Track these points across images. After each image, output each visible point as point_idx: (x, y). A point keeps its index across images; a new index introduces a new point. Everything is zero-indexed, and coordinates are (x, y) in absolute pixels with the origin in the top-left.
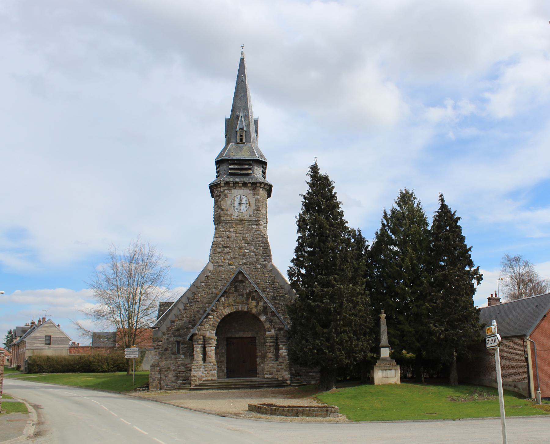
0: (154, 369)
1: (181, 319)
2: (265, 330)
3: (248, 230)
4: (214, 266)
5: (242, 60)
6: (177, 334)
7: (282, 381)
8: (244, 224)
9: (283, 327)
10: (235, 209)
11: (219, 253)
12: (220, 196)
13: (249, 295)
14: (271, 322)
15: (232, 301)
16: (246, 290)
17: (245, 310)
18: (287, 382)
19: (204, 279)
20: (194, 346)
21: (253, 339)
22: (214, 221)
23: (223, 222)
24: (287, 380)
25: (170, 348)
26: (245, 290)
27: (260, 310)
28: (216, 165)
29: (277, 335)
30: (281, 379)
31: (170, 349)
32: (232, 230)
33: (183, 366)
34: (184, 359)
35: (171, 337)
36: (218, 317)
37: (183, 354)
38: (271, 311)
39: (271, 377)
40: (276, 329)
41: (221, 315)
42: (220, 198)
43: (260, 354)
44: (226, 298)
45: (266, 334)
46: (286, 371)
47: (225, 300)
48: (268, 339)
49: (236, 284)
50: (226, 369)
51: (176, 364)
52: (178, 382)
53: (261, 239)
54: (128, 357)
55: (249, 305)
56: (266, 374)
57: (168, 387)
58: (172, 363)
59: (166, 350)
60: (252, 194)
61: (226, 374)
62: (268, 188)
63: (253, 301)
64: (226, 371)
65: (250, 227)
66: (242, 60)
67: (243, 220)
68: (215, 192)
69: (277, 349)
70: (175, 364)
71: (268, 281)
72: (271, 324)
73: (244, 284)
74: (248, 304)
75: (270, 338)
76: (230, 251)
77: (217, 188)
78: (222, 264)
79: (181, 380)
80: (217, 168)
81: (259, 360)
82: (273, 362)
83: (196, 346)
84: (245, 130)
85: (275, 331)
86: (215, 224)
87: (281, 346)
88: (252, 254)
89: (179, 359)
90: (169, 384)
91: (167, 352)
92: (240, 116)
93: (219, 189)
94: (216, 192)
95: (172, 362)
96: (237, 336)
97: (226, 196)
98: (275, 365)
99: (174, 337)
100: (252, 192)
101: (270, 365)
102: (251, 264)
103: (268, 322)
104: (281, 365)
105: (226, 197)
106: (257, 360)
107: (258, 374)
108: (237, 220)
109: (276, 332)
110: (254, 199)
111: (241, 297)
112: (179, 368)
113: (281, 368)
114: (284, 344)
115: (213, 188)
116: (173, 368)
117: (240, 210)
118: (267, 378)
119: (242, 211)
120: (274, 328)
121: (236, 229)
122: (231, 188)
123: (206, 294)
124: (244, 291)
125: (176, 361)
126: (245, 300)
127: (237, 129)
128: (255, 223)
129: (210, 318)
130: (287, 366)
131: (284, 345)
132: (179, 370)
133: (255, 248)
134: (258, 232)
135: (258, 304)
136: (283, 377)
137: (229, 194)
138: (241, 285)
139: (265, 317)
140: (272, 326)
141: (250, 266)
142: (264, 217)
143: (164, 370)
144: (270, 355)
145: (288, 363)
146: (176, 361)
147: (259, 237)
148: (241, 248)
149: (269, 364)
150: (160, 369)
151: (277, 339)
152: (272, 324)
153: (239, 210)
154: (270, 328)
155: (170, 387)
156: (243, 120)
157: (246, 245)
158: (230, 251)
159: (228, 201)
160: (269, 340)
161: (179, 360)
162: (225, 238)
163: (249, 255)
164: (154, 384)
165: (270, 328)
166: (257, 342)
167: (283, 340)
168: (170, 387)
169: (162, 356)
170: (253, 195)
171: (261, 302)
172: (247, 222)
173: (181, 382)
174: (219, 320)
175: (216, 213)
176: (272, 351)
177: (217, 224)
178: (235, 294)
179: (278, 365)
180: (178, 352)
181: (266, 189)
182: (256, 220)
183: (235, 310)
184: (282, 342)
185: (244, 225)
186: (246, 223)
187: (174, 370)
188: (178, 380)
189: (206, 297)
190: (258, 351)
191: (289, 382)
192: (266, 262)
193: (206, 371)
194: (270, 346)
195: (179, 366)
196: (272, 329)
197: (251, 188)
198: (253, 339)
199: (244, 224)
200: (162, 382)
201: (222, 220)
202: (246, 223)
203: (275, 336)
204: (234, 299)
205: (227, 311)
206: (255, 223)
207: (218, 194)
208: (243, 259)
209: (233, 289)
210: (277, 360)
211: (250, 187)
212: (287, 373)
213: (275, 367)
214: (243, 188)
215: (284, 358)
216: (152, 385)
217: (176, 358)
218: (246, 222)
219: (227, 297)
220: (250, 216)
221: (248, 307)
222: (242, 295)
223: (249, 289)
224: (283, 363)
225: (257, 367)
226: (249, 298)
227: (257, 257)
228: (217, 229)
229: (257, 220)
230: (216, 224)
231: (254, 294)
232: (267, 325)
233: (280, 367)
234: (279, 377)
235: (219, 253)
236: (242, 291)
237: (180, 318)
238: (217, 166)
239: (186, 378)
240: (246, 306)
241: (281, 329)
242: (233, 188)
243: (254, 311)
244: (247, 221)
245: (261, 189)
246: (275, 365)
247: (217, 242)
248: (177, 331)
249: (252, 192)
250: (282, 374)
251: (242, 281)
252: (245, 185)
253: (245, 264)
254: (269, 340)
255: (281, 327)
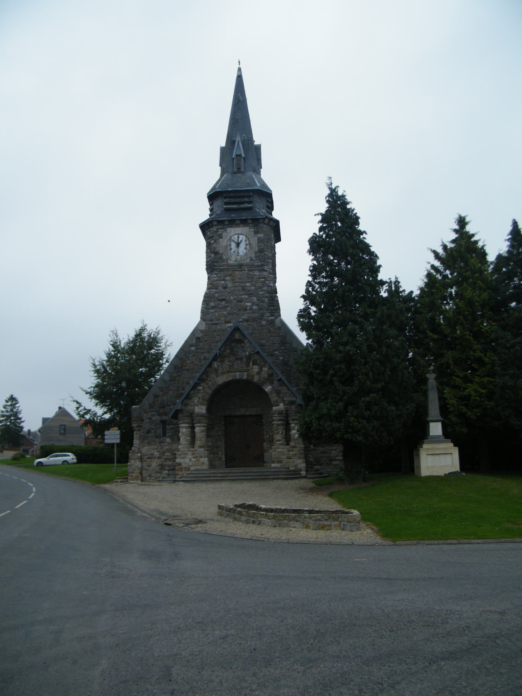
0: (134, 456)
1: (166, 393)
2: (272, 406)
3: (248, 278)
4: (206, 324)
5: (239, 79)
6: (161, 411)
7: (294, 471)
8: (243, 270)
9: (295, 400)
10: (232, 251)
11: (213, 308)
12: (213, 237)
13: (249, 358)
14: (278, 393)
15: (227, 367)
16: (245, 352)
17: (244, 378)
18: (302, 472)
19: (194, 342)
20: (180, 426)
21: (259, 417)
22: (207, 269)
23: (217, 269)
24: (301, 470)
25: (153, 429)
26: (244, 352)
27: (264, 378)
28: (209, 201)
29: (287, 410)
30: (293, 469)
31: (153, 431)
32: (228, 278)
33: (170, 452)
34: (170, 443)
35: (154, 415)
36: (209, 388)
37: (170, 437)
38: (279, 378)
39: (280, 467)
40: (286, 402)
41: (213, 385)
42: (212, 240)
43: (268, 436)
44: (219, 363)
45: (272, 410)
46: (299, 458)
47: (218, 366)
48: (276, 415)
49: (233, 345)
50: (224, 456)
51: (161, 450)
52: (164, 472)
53: (265, 288)
54: (109, 442)
55: (250, 372)
56: (273, 462)
57: (152, 478)
58: (156, 449)
59: (149, 432)
60: (253, 233)
61: (224, 462)
62: (274, 225)
63: (254, 367)
64: (224, 459)
65: (251, 273)
66: (239, 79)
67: (243, 265)
68: (207, 234)
69: (288, 429)
70: (159, 449)
71: (277, 341)
72: (279, 397)
73: (243, 345)
74: (248, 371)
75: (278, 414)
76: (227, 304)
77: (209, 227)
78: (217, 322)
79: (167, 470)
80: (211, 205)
81: (267, 444)
82: (282, 447)
83: (182, 425)
84: (243, 156)
85: (284, 405)
86: (208, 273)
87: (293, 425)
88: (254, 307)
89: (164, 443)
90: (153, 475)
91: (150, 434)
92: (237, 141)
93: (212, 229)
94: (209, 233)
95: (156, 447)
96: (238, 413)
97: (221, 236)
98: (284, 450)
99: (159, 415)
100: (253, 230)
101: (278, 450)
102: (254, 320)
103: (275, 394)
104: (293, 451)
105: (220, 238)
106: (265, 444)
107: (266, 462)
108: (235, 266)
109: (285, 406)
110: (256, 238)
111: (239, 362)
112: (165, 454)
113: (293, 455)
114: (296, 422)
115: (205, 227)
116: (157, 454)
117: (238, 253)
118: (275, 468)
119: (241, 253)
120: (284, 402)
121: (233, 277)
122: (226, 227)
123: (197, 360)
124: (243, 355)
125: (161, 445)
126: (244, 365)
127: (234, 156)
128: (258, 268)
129: (199, 390)
130: (301, 451)
131: (296, 424)
132: (165, 457)
133: (258, 300)
134: (261, 280)
135: (261, 369)
136: (296, 466)
137: (224, 235)
138: (239, 345)
139: (270, 387)
140: (280, 399)
141: (252, 324)
142: (269, 260)
143: (146, 457)
144: (278, 437)
145: (302, 447)
146: (161, 445)
147: (264, 286)
148: (241, 301)
149: (277, 448)
150: (141, 456)
151: (287, 416)
152: (281, 395)
153: (236, 253)
154: (277, 401)
155: (153, 478)
156: (241, 145)
157: (247, 296)
158: (227, 304)
159: (223, 242)
160: (276, 417)
161: (165, 444)
162: (220, 289)
163: (251, 309)
164: (134, 475)
165: (277, 401)
166: (264, 421)
167: (295, 417)
168: (153, 478)
169: (144, 440)
170: (254, 234)
171: (265, 367)
172: (247, 268)
173: (167, 472)
174: (211, 392)
175: (208, 259)
176: (281, 432)
177: (210, 272)
178: (231, 357)
179: (289, 451)
180: (164, 435)
181: (271, 226)
182: (259, 264)
183: (231, 379)
184: (293, 420)
185: (243, 272)
186: (246, 269)
187: (159, 458)
188: (164, 470)
189: (197, 364)
190: (265, 433)
191: (303, 473)
192: (273, 318)
193: (194, 458)
194: (278, 425)
195: (164, 453)
196: (280, 402)
197: (251, 225)
198: (259, 417)
199: (243, 270)
200: (144, 472)
201: (215, 266)
202: (246, 269)
203: (284, 412)
204: (229, 364)
205: (221, 380)
206: (258, 268)
207: (211, 235)
208: (244, 315)
209: (228, 351)
210: (288, 444)
211: (250, 223)
212: (300, 461)
213: (286, 453)
214: (241, 225)
215: (296, 441)
216: (131, 476)
217: (161, 442)
218: (246, 267)
219: (220, 362)
220: (251, 260)
221: (247, 374)
222: (241, 359)
223: (249, 350)
224: (296, 447)
225: (265, 454)
226: (250, 363)
227: (261, 312)
228: (210, 278)
229: (261, 265)
230: (209, 272)
231: (256, 357)
232: (274, 398)
233: (291, 453)
234: (290, 466)
235: (213, 308)
236: (240, 353)
237: (165, 392)
238: (211, 203)
239: (173, 467)
240: (246, 373)
241: (292, 403)
242: (229, 227)
243: (256, 379)
244: (248, 267)
245: (265, 226)
246: (284, 450)
247: (211, 294)
248: (162, 408)
249: (253, 230)
250: (294, 462)
251: (240, 341)
252: (244, 222)
253: (247, 321)
254: (276, 417)
255: (292, 399)
